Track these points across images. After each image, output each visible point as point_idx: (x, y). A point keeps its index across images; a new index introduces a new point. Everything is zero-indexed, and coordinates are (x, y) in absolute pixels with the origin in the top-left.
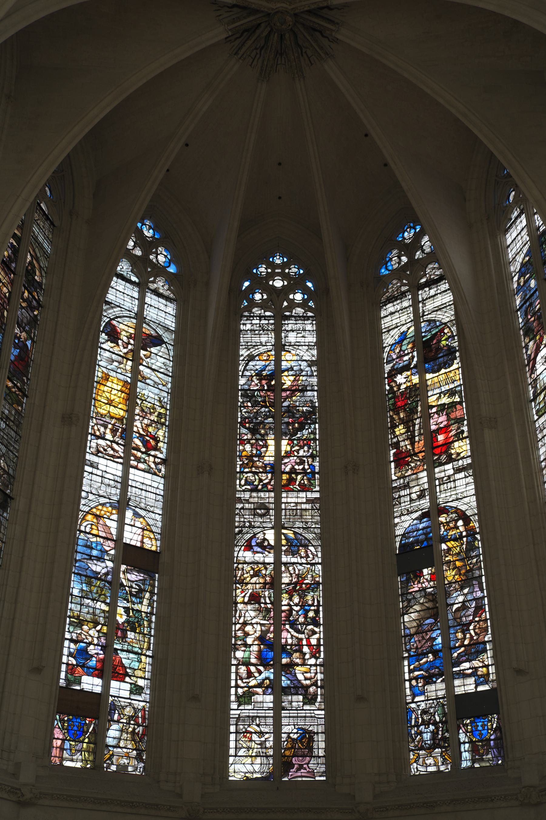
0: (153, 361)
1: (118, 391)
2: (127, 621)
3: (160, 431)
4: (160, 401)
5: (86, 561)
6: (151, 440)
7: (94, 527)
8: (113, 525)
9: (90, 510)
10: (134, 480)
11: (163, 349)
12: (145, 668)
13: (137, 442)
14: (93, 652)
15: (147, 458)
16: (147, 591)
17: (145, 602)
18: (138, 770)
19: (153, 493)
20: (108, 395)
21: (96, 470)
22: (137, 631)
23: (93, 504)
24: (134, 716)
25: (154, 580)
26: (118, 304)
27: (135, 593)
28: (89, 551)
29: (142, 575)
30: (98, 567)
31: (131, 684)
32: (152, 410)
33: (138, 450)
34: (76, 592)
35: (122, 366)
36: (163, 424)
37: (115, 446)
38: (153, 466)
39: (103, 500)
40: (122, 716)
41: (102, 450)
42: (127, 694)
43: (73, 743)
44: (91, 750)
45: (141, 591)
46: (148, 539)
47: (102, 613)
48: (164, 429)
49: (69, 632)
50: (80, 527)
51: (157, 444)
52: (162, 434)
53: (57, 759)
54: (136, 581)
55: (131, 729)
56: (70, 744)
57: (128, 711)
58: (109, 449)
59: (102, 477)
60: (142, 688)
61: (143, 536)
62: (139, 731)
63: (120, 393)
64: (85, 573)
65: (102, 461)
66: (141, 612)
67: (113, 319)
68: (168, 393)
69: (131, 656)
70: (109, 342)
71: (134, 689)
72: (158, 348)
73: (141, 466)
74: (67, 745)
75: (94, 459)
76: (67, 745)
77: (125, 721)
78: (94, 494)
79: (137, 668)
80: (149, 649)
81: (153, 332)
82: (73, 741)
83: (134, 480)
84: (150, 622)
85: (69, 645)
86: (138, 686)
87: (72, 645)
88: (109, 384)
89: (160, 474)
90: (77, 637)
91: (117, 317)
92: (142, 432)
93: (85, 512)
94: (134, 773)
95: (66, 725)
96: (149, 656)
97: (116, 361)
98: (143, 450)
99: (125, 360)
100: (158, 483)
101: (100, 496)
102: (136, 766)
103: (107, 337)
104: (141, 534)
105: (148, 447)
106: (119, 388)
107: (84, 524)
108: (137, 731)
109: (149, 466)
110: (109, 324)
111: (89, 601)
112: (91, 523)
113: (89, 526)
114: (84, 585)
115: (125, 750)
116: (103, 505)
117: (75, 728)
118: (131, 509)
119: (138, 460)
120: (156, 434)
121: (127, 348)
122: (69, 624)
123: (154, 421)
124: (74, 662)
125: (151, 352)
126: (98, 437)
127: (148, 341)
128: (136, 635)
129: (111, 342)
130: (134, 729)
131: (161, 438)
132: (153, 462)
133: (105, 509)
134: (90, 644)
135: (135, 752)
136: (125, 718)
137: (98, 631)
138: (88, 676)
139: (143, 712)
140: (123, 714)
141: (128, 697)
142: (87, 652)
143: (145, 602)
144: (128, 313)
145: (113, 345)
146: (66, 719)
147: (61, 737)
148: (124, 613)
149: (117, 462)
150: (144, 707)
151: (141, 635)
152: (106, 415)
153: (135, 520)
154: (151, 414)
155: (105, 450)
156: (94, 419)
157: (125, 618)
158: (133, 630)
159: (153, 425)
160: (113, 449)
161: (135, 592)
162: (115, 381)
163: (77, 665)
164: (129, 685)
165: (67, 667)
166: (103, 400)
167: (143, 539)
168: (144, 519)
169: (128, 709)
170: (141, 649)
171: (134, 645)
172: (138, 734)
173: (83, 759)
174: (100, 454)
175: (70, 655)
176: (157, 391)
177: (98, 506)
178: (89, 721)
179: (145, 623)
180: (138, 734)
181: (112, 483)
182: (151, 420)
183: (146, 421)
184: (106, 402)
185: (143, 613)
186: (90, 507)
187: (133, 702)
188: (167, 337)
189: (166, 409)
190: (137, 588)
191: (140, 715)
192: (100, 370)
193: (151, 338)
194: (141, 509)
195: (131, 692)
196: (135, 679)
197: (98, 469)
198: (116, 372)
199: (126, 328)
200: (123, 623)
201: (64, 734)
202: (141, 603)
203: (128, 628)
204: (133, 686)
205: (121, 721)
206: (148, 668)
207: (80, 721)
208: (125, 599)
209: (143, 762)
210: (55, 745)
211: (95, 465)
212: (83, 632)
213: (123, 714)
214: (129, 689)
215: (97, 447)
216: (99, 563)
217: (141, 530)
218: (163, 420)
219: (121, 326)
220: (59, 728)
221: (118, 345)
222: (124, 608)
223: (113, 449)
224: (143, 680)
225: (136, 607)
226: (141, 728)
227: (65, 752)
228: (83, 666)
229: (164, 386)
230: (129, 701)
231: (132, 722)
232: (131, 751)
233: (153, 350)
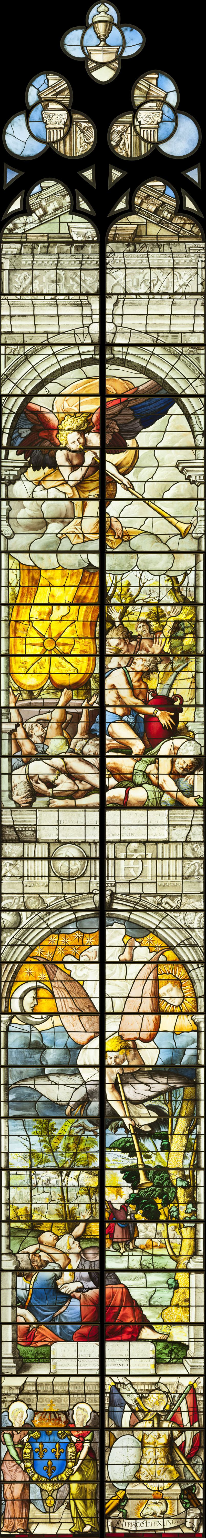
0: (145, 474)
1: (69, 604)
2: (135, 1200)
3: (182, 675)
4: (176, 589)
5: (31, 1082)
6: (159, 713)
7: (42, 993)
8: (88, 974)
9: (28, 955)
10: (120, 841)
11: (175, 417)
12: (188, 1300)
13: (121, 731)
14: (73, 1287)
15: (151, 769)
16: (180, 1116)
17: (177, 1143)
18: (188, 1525)
19: (177, 859)
20: (42, 627)
21: (32, 846)
22: (162, 1217)
23: (33, 937)
24: (170, 1411)
25: (196, 1084)
26: (41, 339)
27: (149, 1129)
28: (38, 1056)
29: (164, 1080)
30: (60, 1090)
31: (154, 1341)
32: (154, 625)
33: (127, 752)
34: (16, 1161)
35: (70, 528)
36: (187, 654)
37: (75, 764)
38: (169, 784)
39: (56, 920)
40: (140, 1415)
41: (43, 786)
42: (148, 1366)
43: (48, 1487)
44: (89, 1497)
45: (163, 1119)
46: (170, 985)
47: (83, 1194)
48: (192, 666)
49: (11, 1254)
50: (8, 1004)
51: (176, 718)
52: (187, 684)
53: (16, 1522)
54: (150, 1098)
55: (163, 1440)
56: (42, 1490)
57: (156, 1402)
58: (63, 777)
59: (49, 859)
60: (184, 1347)
61: (156, 980)
62: (185, 1442)
63: (74, 608)
64: (33, 1113)
65: (47, 817)
66: (166, 1170)
67: (34, 393)
68: (196, 553)
69: (153, 1278)
70: (30, 469)
71: (166, 1351)
72: (159, 424)
73: (137, 794)
74: (35, 1492)
75: (26, 818)
76: (35, 1492)
77: (148, 1425)
78: (33, 911)
79: (168, 1303)
80: (195, 1254)
81: (141, 382)
82: (45, 1482)
83: (120, 841)
84: (191, 1187)
85: (15, 1283)
86: (174, 1343)
87: (21, 1282)
88: (42, 595)
89: (191, 802)
90: (32, 1262)
91: (43, 383)
92: (130, 700)
93: (15, 962)
94: (179, 1531)
95: (28, 1451)
96: (197, 1271)
97: (54, 519)
98: (138, 746)
99: (79, 504)
100: (189, 825)
101: (48, 911)
102: (183, 1516)
103: (22, 457)
104: (151, 977)
105: (152, 734)
106: (69, 595)
107: (18, 994)
108: (178, 1442)
109: (160, 787)
110: (25, 412)
111: (50, 1173)
112: (33, 984)
113: (32, 994)
114: (35, 1139)
115: (154, 1486)
116: (58, 930)
117: (48, 1455)
118: (119, 919)
119: (127, 781)
120: (170, 688)
121: (80, 465)
122: (8, 1237)
123: (162, 654)
124: (31, 1318)
125: (138, 448)
126: (29, 758)
127: (127, 417)
128: (161, 1227)
129: (36, 468)
130: (171, 1440)
131: (187, 696)
132: (170, 774)
133: (63, 940)
134: (63, 1270)
135: (177, 1488)
136: (148, 1418)
137: (78, 1239)
138: (66, 1341)
139: (190, 1398)
140: (142, 1411)
141: (152, 1372)
142: (56, 1290)
143: (177, 1143)
144: (75, 351)
145: (40, 474)
146: (26, 1439)
147: (20, 1477)
148: (124, 1183)
149: (86, 808)
150: (192, 1386)
151: (171, 1226)
152: (41, 689)
153: (131, 946)
154: (153, 636)
155: (51, 785)
156: (13, 712)
157: (127, 1192)
158: (152, 1217)
159: (161, 667)
160: (72, 776)
161: (150, 1125)
162: (57, 578)
163: (38, 1323)
164: (152, 1346)
165: (15, 1331)
166: (30, 650)
167: (157, 987)
168: (157, 935)
169: (154, 1397)
170: (175, 1257)
171: (157, 1251)
172: (182, 1448)
173: (74, 1515)
174: (40, 802)
175: (19, 1302)
176: (163, 562)
177: (46, 936)
178: (78, 1436)
179: (181, 1193)
180: (182, 1448)
181: (76, 866)
182: (153, 655)
183: (140, 664)
184: (38, 650)
185: (171, 1172)
186: (27, 945)
187: (163, 1380)
188: (181, 375)
189: (195, 604)
190: (154, 1114)
191: (184, 1407)
192: (13, 564)
193: (134, 402)
194: (147, 910)
195: (158, 1361)
196: (165, 1329)
197: (37, 841)
198: (57, 552)
199: (71, 404)
200: (124, 1207)
201: (25, 1470)
202: (166, 1148)
203: (139, 1216)
204: (161, 1345)
205: (140, 1425)
206: (197, 1297)
207: (57, 1439)
208: (124, 1150)
209: (198, 1506)
210: (9, 1496)
211: (29, 833)
212: (42, 1247)
213: (142, 1411)
214: (152, 1355)
215: (30, 784)
216: (64, 1079)
217: (152, 966)
218: (188, 642)
219: (60, 404)
220: (14, 1460)
221: (54, 466)
222: (123, 1170)
223: (72, 776)
224: (185, 1328)
225: (154, 1162)
226: (189, 1435)
227: (32, 1506)
228: (51, 1323)
229: (183, 535)
230: (155, 1380)
231: (166, 1425)
232: (167, 1485)
233: (145, 438)
